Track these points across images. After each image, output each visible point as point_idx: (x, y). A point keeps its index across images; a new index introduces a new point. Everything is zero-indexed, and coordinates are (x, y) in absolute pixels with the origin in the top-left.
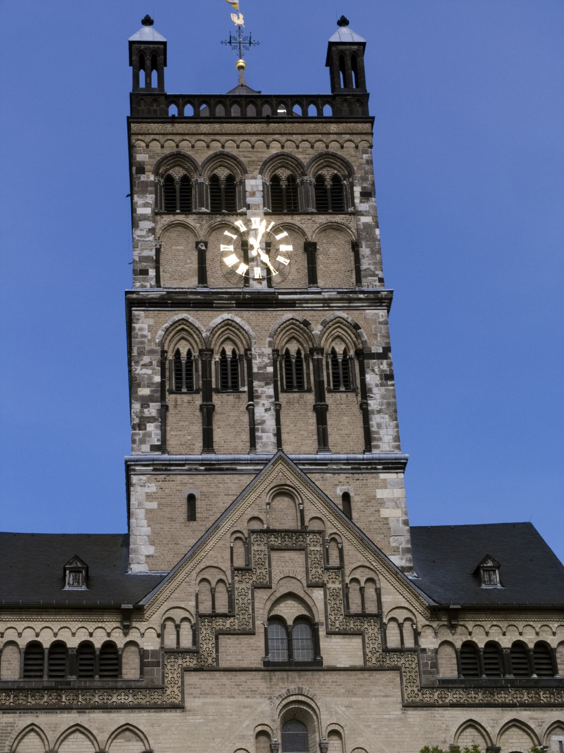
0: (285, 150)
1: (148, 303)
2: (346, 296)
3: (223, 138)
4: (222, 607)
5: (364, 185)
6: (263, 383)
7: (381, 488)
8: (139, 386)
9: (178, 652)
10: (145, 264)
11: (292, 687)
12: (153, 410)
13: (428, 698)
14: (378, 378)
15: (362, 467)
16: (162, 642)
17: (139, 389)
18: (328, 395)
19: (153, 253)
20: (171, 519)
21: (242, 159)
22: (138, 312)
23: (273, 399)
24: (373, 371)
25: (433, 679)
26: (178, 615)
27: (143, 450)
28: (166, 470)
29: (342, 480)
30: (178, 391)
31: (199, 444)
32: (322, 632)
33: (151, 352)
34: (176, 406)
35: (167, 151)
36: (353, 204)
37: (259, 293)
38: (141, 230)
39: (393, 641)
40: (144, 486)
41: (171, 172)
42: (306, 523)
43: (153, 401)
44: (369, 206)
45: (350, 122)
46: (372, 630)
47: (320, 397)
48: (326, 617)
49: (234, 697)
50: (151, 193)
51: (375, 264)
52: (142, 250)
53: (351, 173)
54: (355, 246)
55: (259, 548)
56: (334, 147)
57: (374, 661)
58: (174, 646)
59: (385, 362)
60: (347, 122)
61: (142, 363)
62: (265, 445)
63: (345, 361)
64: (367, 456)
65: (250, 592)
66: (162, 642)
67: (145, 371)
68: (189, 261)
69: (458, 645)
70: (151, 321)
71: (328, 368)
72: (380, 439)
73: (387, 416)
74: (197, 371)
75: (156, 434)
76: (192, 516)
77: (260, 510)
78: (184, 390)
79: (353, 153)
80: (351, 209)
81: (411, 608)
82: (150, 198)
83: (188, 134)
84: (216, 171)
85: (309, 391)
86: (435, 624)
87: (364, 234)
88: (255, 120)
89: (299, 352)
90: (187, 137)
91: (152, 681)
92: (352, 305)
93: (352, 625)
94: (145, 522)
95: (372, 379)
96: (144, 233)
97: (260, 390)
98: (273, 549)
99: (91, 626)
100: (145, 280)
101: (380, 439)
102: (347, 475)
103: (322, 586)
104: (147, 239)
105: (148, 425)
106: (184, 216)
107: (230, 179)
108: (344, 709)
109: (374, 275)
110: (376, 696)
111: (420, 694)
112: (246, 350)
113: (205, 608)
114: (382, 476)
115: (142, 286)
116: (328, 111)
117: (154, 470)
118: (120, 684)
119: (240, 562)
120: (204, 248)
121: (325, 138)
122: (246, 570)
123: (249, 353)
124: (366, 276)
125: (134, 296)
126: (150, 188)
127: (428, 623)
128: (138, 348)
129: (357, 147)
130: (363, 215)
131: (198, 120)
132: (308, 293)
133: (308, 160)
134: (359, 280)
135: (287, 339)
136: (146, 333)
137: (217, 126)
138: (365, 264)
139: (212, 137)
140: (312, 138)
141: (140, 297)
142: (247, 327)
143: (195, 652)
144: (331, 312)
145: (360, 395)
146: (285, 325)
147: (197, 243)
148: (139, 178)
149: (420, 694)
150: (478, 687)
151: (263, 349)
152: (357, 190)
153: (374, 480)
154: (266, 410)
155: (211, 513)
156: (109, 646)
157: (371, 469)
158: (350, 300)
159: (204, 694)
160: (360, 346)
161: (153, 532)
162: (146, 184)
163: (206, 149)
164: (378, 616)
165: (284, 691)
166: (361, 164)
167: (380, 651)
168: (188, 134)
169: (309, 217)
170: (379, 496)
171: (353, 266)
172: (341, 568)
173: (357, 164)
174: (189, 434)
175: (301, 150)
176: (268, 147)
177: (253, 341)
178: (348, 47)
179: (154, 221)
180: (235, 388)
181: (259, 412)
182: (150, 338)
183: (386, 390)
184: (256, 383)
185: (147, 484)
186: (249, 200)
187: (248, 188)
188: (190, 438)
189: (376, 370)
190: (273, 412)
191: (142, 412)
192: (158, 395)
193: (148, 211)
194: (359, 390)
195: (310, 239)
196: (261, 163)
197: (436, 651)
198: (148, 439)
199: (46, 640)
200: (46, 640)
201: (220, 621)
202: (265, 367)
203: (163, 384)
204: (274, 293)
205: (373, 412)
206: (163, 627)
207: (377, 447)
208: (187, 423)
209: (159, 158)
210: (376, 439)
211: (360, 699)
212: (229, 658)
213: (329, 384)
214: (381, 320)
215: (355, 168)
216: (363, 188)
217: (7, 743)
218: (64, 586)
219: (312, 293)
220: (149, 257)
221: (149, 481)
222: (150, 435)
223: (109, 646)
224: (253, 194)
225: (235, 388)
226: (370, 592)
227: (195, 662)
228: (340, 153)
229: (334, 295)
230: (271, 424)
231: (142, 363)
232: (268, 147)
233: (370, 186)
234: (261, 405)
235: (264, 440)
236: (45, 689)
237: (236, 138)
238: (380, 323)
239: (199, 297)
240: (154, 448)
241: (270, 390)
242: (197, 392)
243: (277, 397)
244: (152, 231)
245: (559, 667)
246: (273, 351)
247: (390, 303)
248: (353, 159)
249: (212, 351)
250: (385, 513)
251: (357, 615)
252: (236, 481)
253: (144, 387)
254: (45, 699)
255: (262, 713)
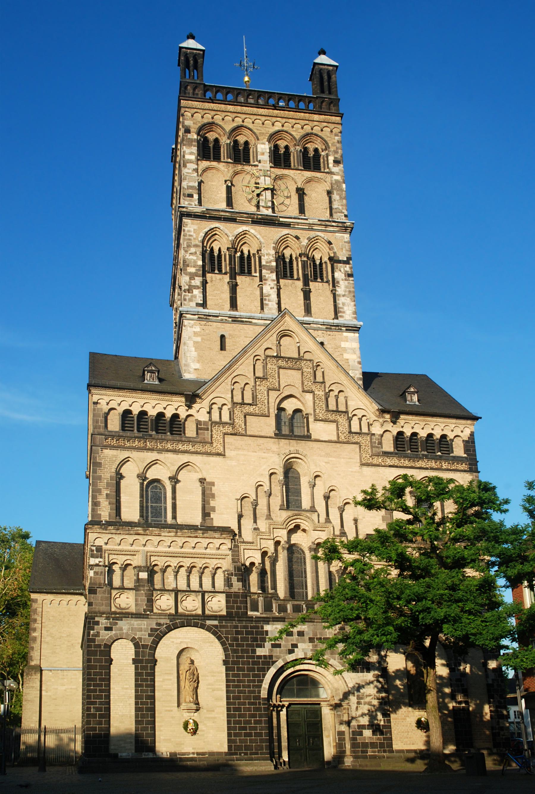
0: (284, 128)
1: (194, 215)
2: (323, 223)
3: (244, 116)
4: (248, 399)
5: (336, 156)
6: (269, 272)
7: (344, 341)
8: (188, 266)
9: (220, 423)
10: (191, 191)
11: (292, 449)
12: (198, 281)
13: (376, 461)
14: (343, 275)
15: (333, 328)
16: (210, 417)
17: (188, 268)
18: (311, 283)
19: (196, 184)
20: (210, 349)
21: (255, 131)
22: (185, 220)
23: (276, 282)
24: (340, 270)
25: (379, 451)
26: (220, 402)
27: (191, 305)
28: (206, 318)
29: (319, 334)
30: (212, 271)
31: (228, 305)
32: (311, 419)
33: (196, 246)
34: (212, 281)
35: (205, 121)
36: (328, 168)
37: (267, 215)
38: (188, 169)
39: (355, 428)
40: (192, 327)
41: (207, 135)
42: (302, 355)
43: (197, 276)
44: (339, 170)
45: (327, 115)
46: (342, 420)
47: (306, 283)
48: (315, 410)
49: (256, 452)
50: (194, 146)
51: (342, 205)
52: (189, 182)
53: (327, 148)
54: (329, 193)
55: (272, 367)
56: (317, 130)
57: (343, 438)
58: (218, 420)
59: (348, 266)
60: (325, 115)
61: (190, 252)
62: (270, 309)
63: (321, 264)
64: (336, 321)
65: (266, 392)
66: (210, 417)
67: (191, 257)
68: (220, 192)
69: (395, 433)
70: (196, 227)
71: (310, 267)
72: (344, 312)
73: (349, 299)
74: (225, 261)
75: (200, 297)
76: (223, 347)
77: (273, 344)
78: (216, 272)
79: (329, 135)
80: (327, 170)
81: (367, 410)
82: (194, 149)
83: (220, 111)
84: (237, 138)
85: (298, 279)
86: (381, 420)
87: (336, 186)
88: (265, 107)
89: (291, 256)
90: (219, 113)
91: (204, 439)
92: (327, 229)
93: (331, 417)
94: (193, 349)
95: (338, 275)
96: (190, 171)
97: (267, 276)
98: (280, 368)
99: (165, 404)
100: (191, 200)
101: (344, 312)
102: (323, 332)
103: (312, 392)
104: (192, 175)
105: (194, 290)
106: (217, 163)
107: (247, 143)
108: (324, 464)
109: (342, 212)
110: (344, 458)
111: (371, 459)
112: (258, 251)
113: (238, 399)
114: (345, 334)
115: (189, 204)
116: (311, 106)
117: (199, 318)
118: (184, 439)
119: (259, 374)
120: (230, 184)
121: (311, 123)
122: (264, 378)
123: (260, 252)
124: (336, 213)
125: (184, 210)
126: (193, 143)
127: (377, 419)
128: (187, 243)
129: (332, 131)
130: (334, 174)
131: (227, 103)
132: (299, 219)
133: (299, 136)
134: (331, 215)
135: (284, 246)
136: (192, 233)
137: (239, 107)
138: (335, 205)
139: (236, 115)
140: (303, 122)
141: (188, 211)
142: (258, 236)
143: (232, 424)
144: (314, 232)
145: (331, 285)
146: (283, 237)
147: (226, 181)
148: (187, 136)
149: (371, 459)
150: (406, 457)
151: (269, 251)
152: (331, 159)
153: (339, 336)
154: (271, 288)
155: (236, 347)
156: (175, 416)
157: (339, 329)
158: (326, 226)
159: (237, 449)
160: (332, 255)
161: (199, 355)
162: (191, 140)
163: (231, 122)
164: (346, 412)
165: (287, 452)
166: (334, 143)
167: (347, 433)
168: (220, 111)
169: (299, 172)
170: (342, 346)
171: (328, 206)
172: (323, 382)
173: (331, 142)
174: (221, 299)
175: (294, 129)
176: (273, 125)
177: (263, 245)
178: (326, 67)
179: (198, 165)
180: (250, 273)
181: (266, 289)
182: (195, 237)
183: (348, 283)
184: (264, 271)
185: (194, 326)
186: (260, 157)
187: (259, 150)
188: (221, 301)
189: (342, 270)
190: (275, 290)
191: (190, 282)
192: (201, 272)
193: (193, 157)
194: (331, 282)
195: (299, 186)
196: (268, 135)
197: (382, 436)
198: (194, 299)
199: (136, 410)
200: (136, 410)
201: (247, 407)
202: (270, 262)
203: (203, 266)
204: (277, 217)
205: (339, 296)
206: (211, 409)
207: (341, 317)
208: (219, 292)
209: (200, 125)
210: (341, 312)
211: (334, 459)
212: (252, 429)
213: (311, 277)
214: (346, 240)
215: (330, 145)
216: (335, 158)
217: (113, 467)
218: (144, 380)
219: (302, 219)
220: (194, 186)
221: (195, 324)
222: (195, 297)
223: (175, 416)
224: (263, 154)
225: (250, 273)
226: (341, 399)
227: (231, 430)
228: (320, 134)
229: (316, 221)
230: (274, 297)
231: (190, 252)
232: (273, 125)
233: (339, 157)
234: (268, 285)
235: (270, 306)
236: (136, 437)
237: (252, 117)
238: (345, 242)
239: (227, 214)
240: (198, 305)
241: (274, 276)
242: (226, 273)
243: (278, 282)
244: (196, 170)
245: (454, 449)
246: (276, 253)
247: (351, 230)
248: (329, 139)
249: (236, 249)
250: (346, 356)
251: (333, 411)
252: (252, 329)
253: (191, 267)
254: (137, 443)
255: (274, 462)
